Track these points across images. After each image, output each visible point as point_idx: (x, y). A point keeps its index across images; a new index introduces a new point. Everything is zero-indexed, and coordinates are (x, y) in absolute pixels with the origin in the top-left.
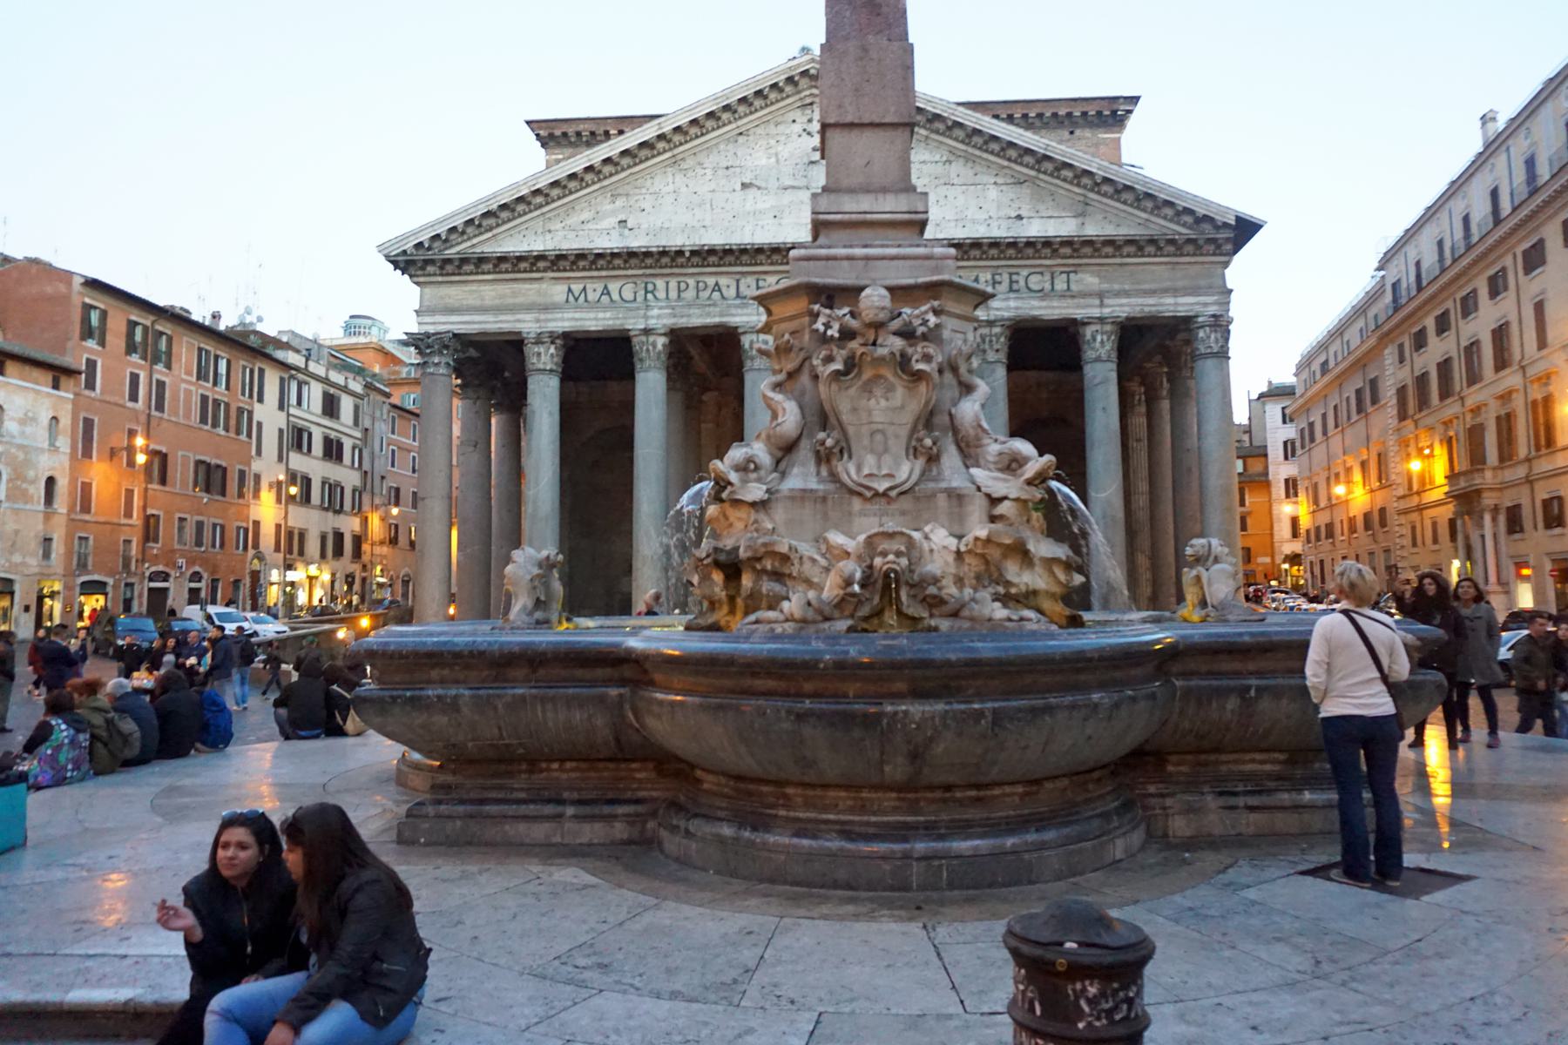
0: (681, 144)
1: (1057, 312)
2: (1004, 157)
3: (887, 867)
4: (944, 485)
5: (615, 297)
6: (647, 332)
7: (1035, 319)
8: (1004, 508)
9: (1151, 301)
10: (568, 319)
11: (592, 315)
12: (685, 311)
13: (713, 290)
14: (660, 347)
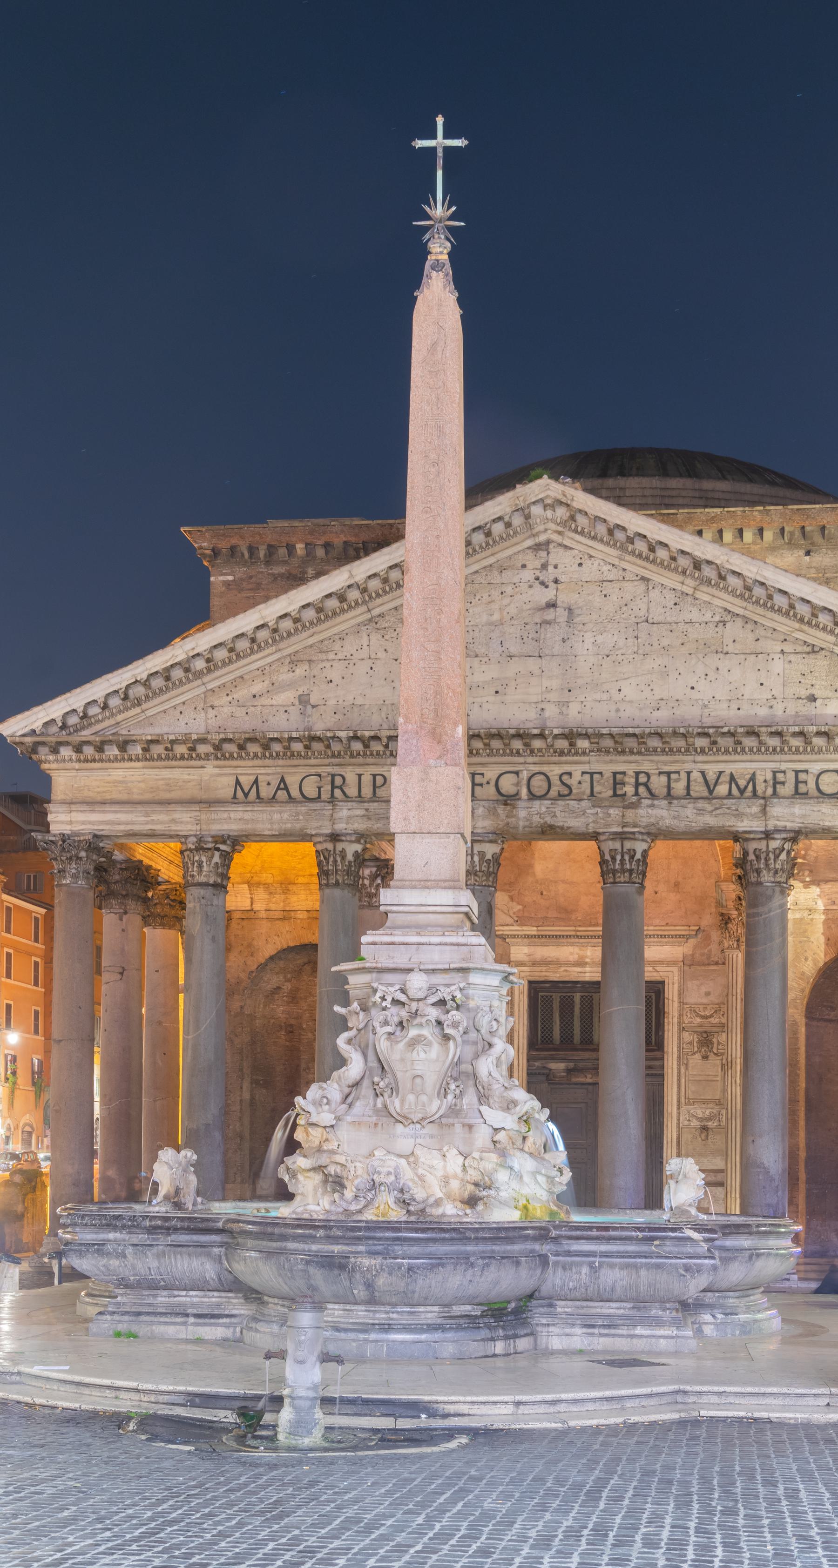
3: (354, 1344)
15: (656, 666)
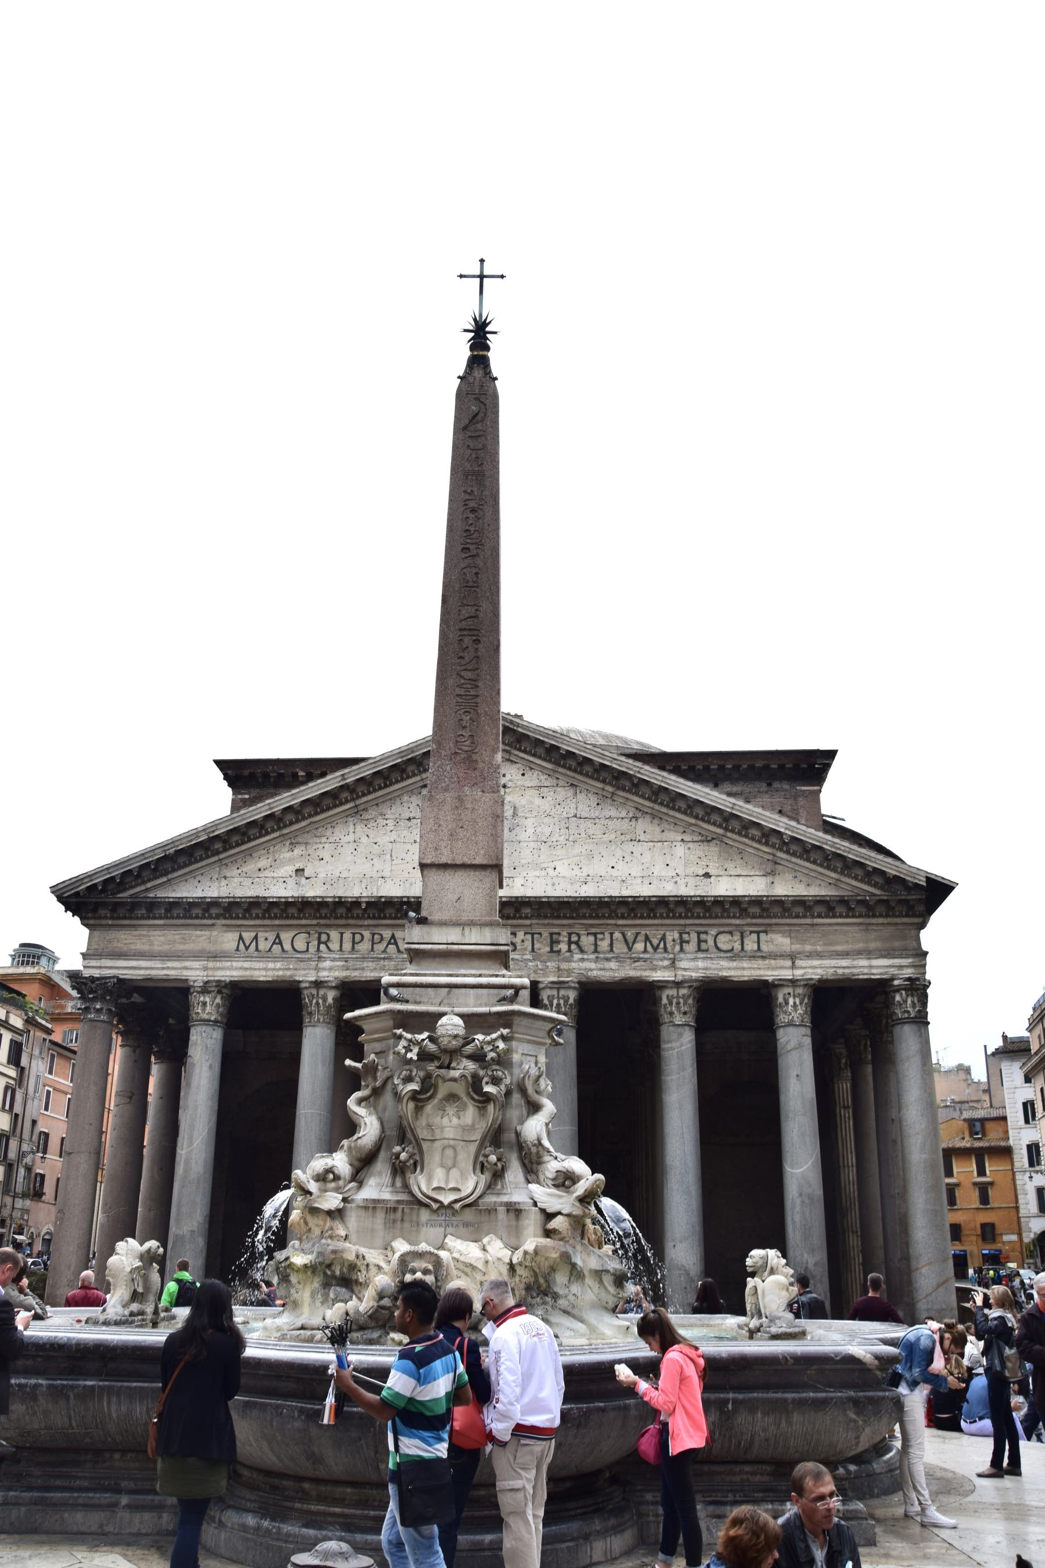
0: (364, 795)
1: (746, 973)
2: (691, 815)
4: (505, 1199)
5: (287, 946)
6: (318, 984)
7: (725, 980)
8: (558, 1223)
9: (844, 963)
10: (236, 969)
11: (261, 965)
12: (359, 964)
13: (389, 943)
14: (330, 1000)
15: (583, 851)
